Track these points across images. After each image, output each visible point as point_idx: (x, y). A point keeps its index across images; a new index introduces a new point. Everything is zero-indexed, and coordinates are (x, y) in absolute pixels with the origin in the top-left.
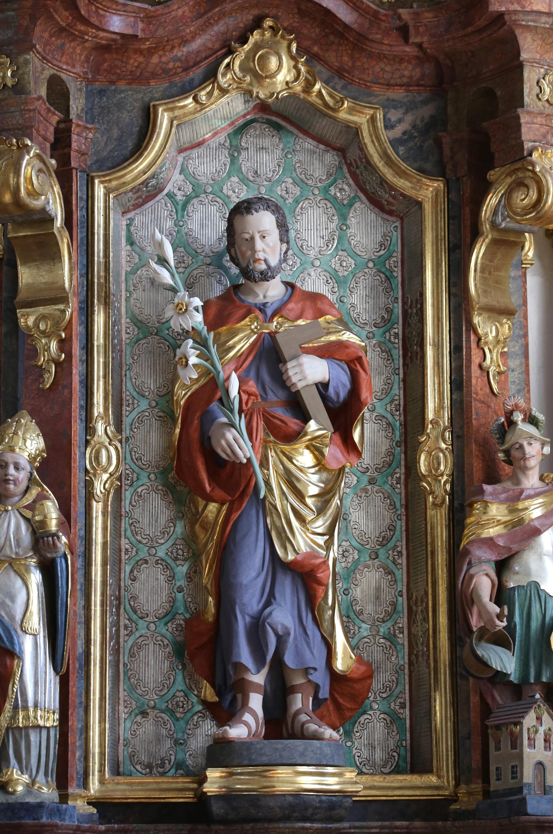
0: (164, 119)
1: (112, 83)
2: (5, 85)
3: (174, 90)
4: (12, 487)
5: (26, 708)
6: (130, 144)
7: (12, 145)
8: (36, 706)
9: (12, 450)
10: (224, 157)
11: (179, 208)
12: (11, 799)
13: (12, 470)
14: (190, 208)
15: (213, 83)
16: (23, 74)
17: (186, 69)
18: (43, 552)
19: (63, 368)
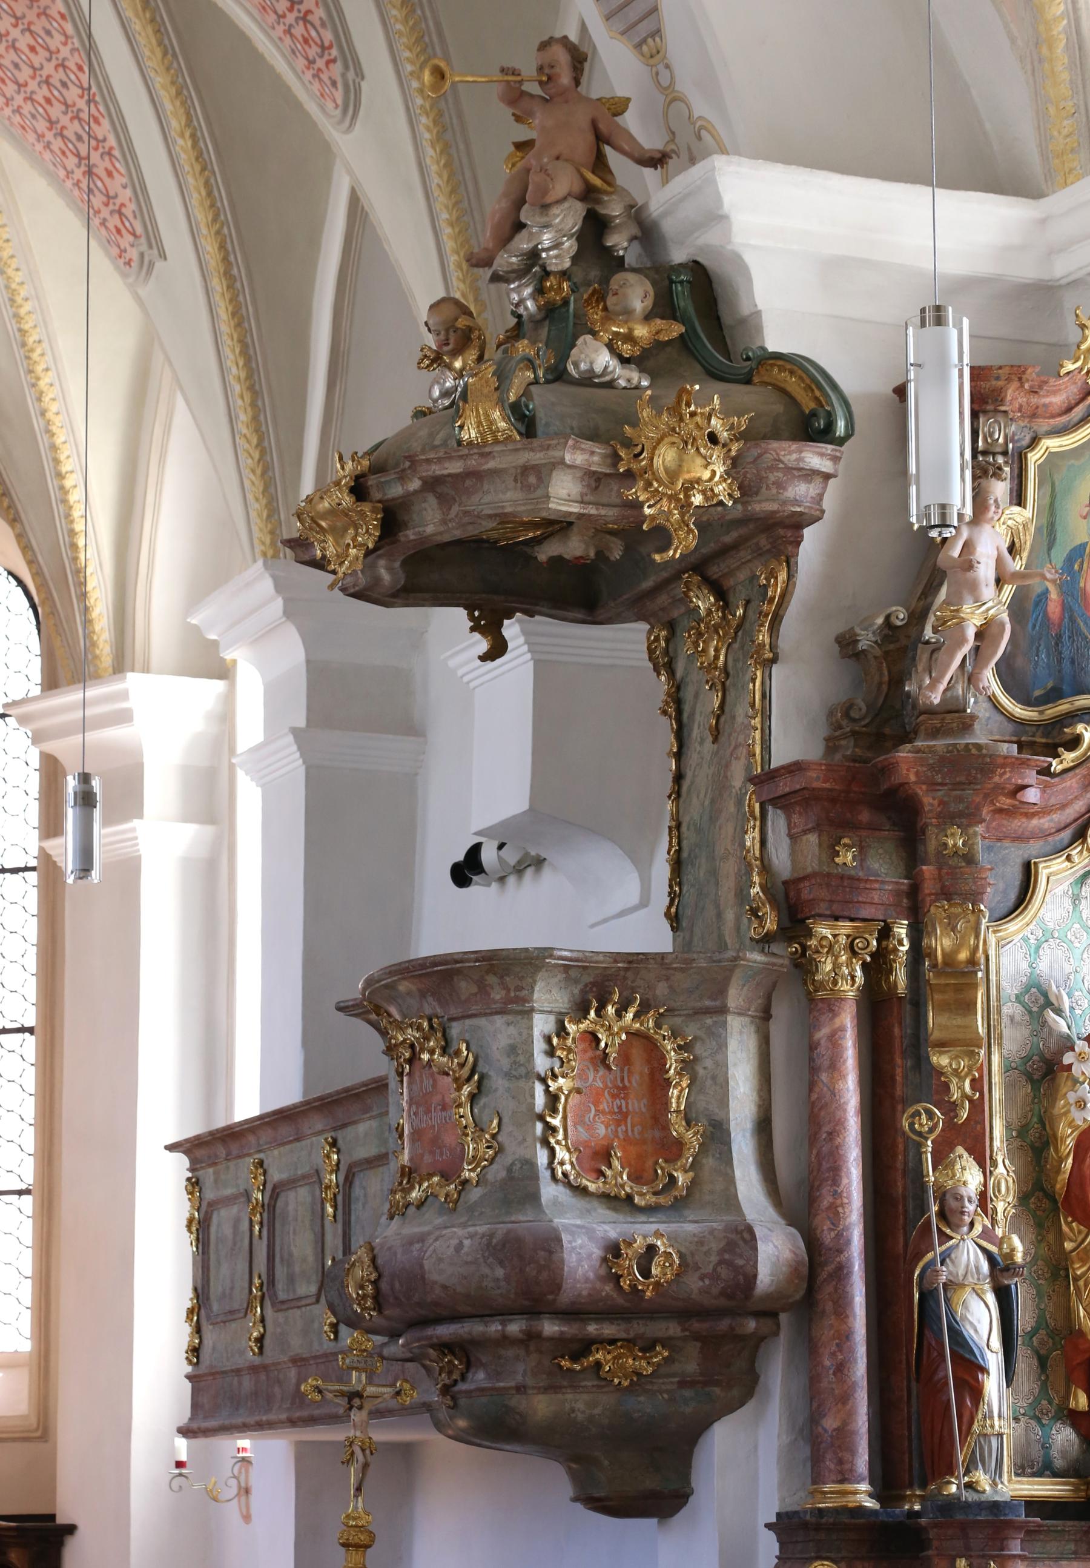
0: (1043, 874)
1: (999, 840)
2: (956, 852)
3: (1048, 848)
4: (966, 1217)
5: (992, 1417)
6: (1013, 896)
7: (968, 909)
8: (1000, 1416)
9: (965, 1183)
10: (1068, 903)
11: (1032, 950)
12: (983, 1498)
13: (967, 1203)
14: (1041, 952)
15: (1083, 843)
16: (973, 844)
17: (1059, 831)
18: (1000, 1279)
19: (977, 1107)
